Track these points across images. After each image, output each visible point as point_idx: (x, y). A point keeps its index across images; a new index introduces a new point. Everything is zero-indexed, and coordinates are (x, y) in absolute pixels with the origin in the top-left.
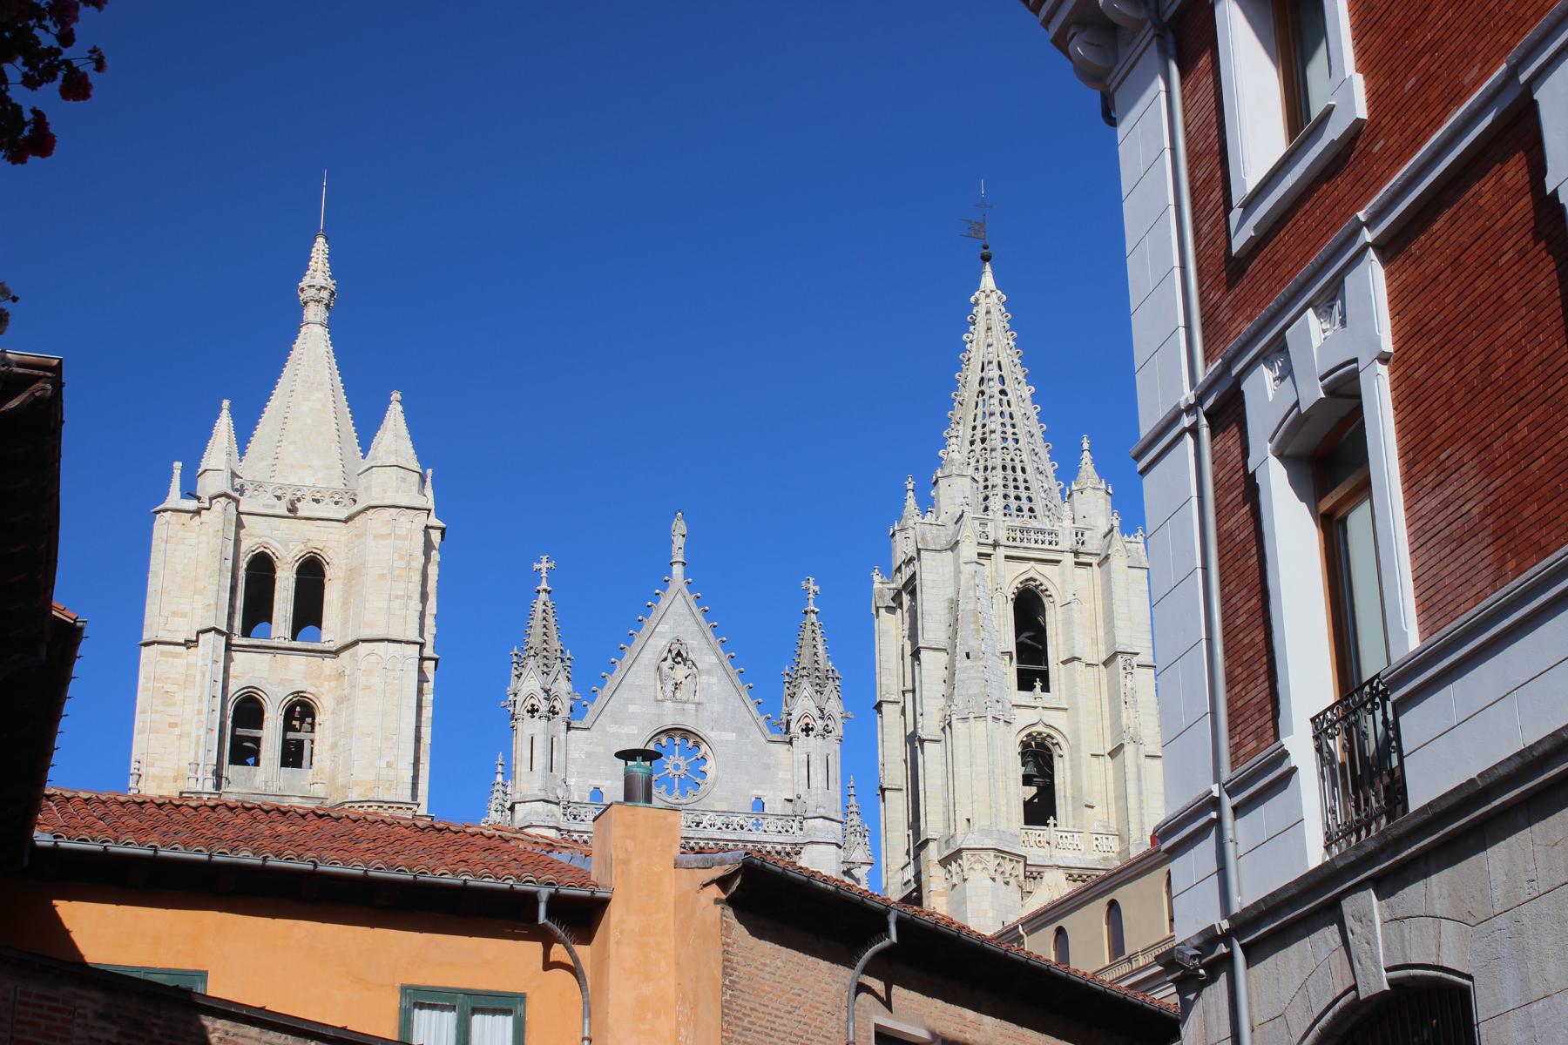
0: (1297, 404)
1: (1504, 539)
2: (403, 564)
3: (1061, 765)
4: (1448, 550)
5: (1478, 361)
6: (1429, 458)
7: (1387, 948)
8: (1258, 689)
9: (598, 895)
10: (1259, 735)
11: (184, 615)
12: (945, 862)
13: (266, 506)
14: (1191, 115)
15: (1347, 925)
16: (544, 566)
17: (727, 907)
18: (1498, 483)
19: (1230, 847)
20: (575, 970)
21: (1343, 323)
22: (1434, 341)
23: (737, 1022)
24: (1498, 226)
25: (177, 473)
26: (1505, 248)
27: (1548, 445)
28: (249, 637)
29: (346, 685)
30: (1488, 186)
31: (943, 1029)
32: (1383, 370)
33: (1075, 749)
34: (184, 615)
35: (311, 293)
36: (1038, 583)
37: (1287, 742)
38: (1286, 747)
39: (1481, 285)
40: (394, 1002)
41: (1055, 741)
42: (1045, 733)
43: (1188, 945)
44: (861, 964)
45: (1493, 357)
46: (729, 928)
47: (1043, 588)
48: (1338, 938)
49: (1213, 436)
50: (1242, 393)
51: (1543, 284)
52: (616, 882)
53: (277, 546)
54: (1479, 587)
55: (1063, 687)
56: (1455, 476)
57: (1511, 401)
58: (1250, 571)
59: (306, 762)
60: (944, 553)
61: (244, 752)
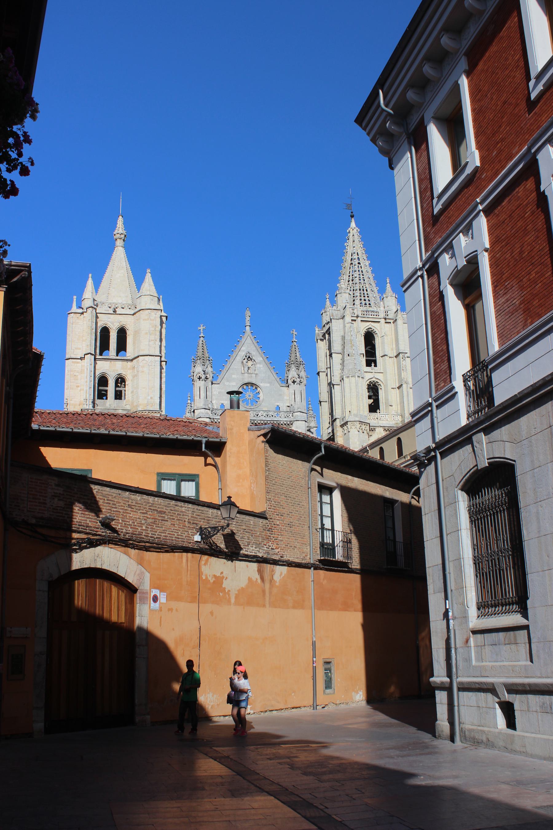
0: (457, 266)
1: (527, 312)
4: (508, 316)
5: (518, 250)
6: (502, 284)
7: (487, 452)
8: (444, 365)
9: (222, 440)
11: (80, 349)
12: (342, 426)
13: (105, 310)
14: (419, 165)
15: (474, 445)
16: (201, 328)
18: (525, 293)
19: (435, 419)
20: (215, 466)
21: (472, 238)
22: (503, 244)
23: (271, 482)
24: (525, 203)
25: (75, 300)
26: (527, 211)
27: (542, 279)
30: (521, 189)
31: (341, 483)
32: (486, 254)
33: (386, 386)
34: (80, 349)
35: (118, 236)
37: (454, 383)
39: (519, 224)
40: (155, 478)
44: (312, 461)
45: (523, 249)
47: (374, 331)
48: (471, 449)
49: (428, 278)
50: (438, 263)
51: (540, 223)
53: (110, 324)
54: (519, 329)
55: (381, 365)
56: (510, 291)
57: (529, 264)
58: (441, 325)
59: (123, 398)
60: (340, 320)
61: (102, 395)
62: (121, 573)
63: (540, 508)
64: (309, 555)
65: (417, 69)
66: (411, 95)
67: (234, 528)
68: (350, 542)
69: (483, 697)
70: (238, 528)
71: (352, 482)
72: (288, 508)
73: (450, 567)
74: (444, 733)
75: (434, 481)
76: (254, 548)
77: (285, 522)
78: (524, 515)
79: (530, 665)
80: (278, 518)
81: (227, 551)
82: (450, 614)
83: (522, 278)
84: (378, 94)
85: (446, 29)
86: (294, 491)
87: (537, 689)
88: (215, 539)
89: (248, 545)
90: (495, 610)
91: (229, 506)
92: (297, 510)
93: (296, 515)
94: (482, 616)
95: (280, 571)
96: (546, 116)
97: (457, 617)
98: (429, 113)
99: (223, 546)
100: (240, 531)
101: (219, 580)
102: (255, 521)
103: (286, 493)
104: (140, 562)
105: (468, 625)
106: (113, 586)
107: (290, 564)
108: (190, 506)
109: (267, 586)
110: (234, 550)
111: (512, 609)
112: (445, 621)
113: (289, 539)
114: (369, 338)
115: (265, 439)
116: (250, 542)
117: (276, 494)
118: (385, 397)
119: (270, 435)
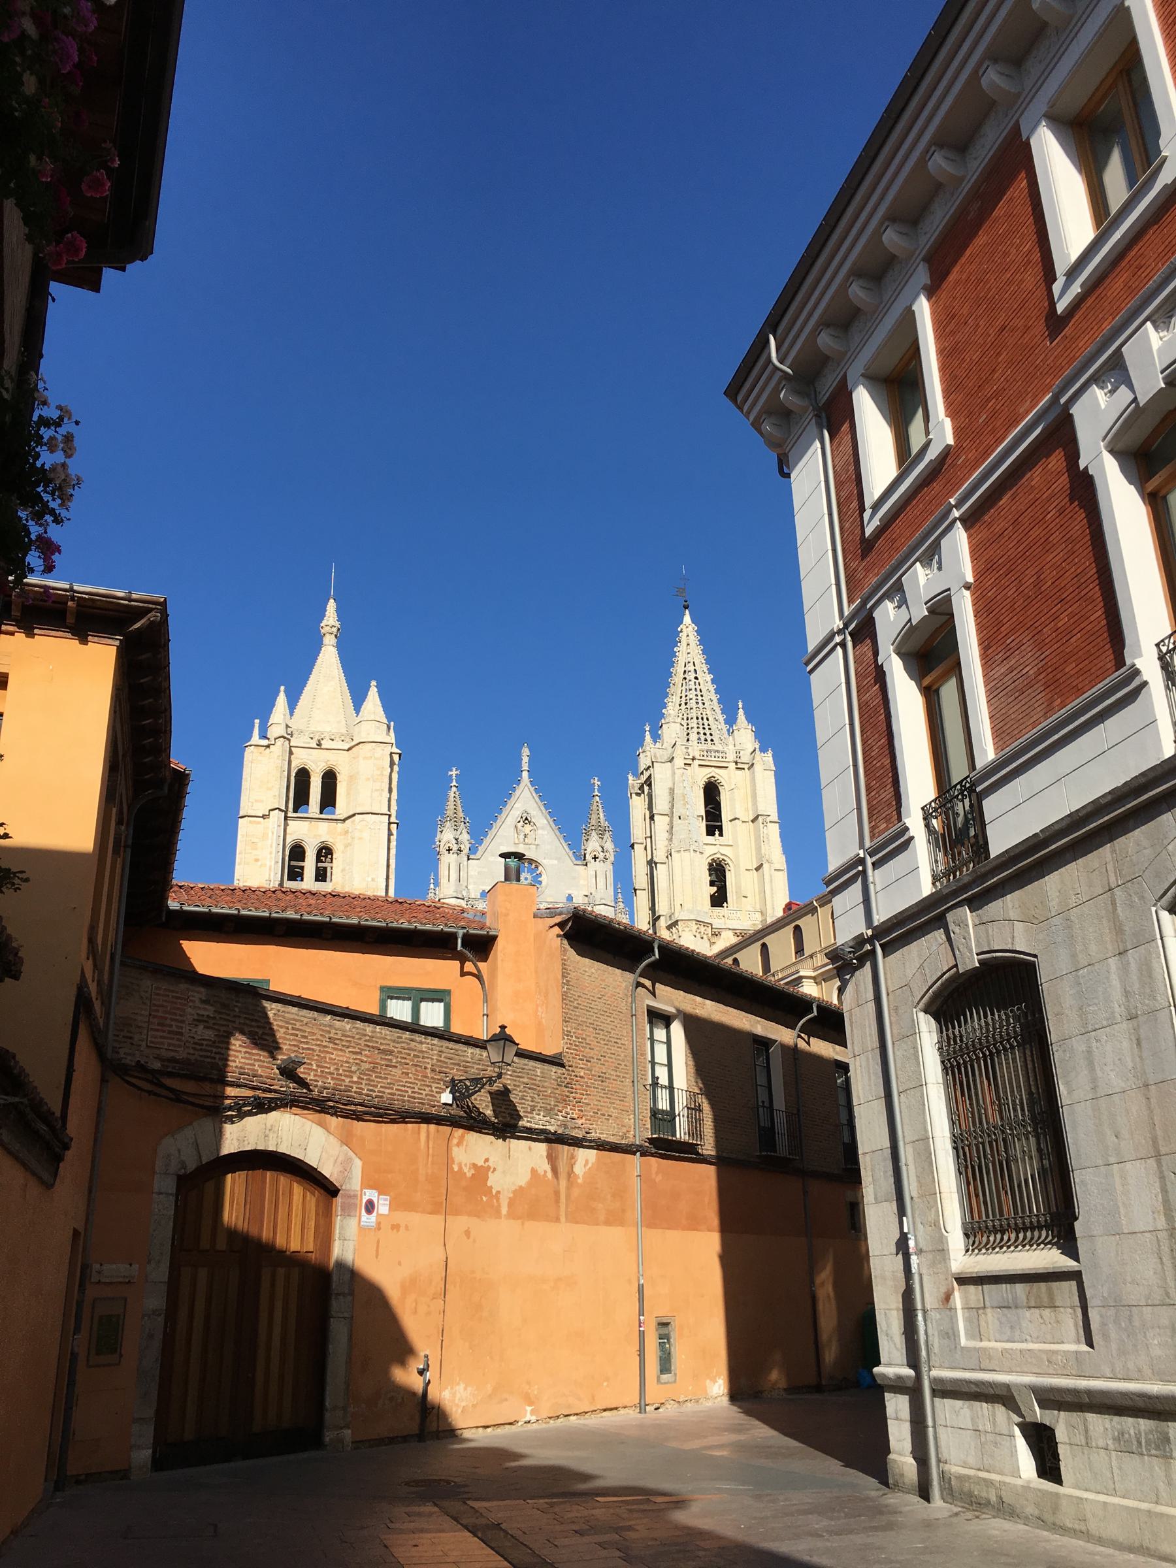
0: (910, 620)
2: (379, 773)
4: (1013, 697)
5: (1031, 580)
6: (1000, 643)
10: (888, 820)
11: (261, 801)
13: (304, 743)
14: (837, 461)
15: (950, 928)
16: (454, 773)
18: (1047, 653)
19: (871, 887)
20: (479, 977)
21: (940, 569)
22: (1001, 572)
26: (1050, 509)
27: (1082, 626)
28: (297, 812)
29: (349, 837)
30: (1037, 473)
31: (684, 1008)
32: (967, 593)
34: (261, 801)
37: (908, 821)
38: (907, 825)
39: (1034, 534)
40: (376, 995)
43: (846, 945)
44: (639, 970)
45: (1042, 577)
46: (565, 950)
48: (944, 937)
49: (854, 647)
51: (1077, 528)
53: (312, 764)
56: (1017, 652)
59: (328, 879)
61: (295, 874)
62: (312, 1159)
63: (1094, 1044)
65: (837, 291)
66: (825, 340)
67: (509, 1082)
69: (985, 1411)
70: (515, 1081)
73: (907, 1154)
74: (906, 1481)
75: (870, 995)
76: (541, 1117)
77: (593, 1073)
78: (1058, 1056)
79: (1088, 1353)
80: (582, 1066)
81: (496, 1121)
82: (911, 1243)
83: (1040, 628)
84: (768, 341)
85: (892, 218)
86: (609, 1019)
87: (1107, 1401)
88: (476, 1099)
90: (1002, 1239)
92: (613, 1052)
94: (973, 1250)
95: (585, 1158)
96: (1086, 338)
97: (924, 1249)
98: (856, 369)
99: (489, 1112)
100: (519, 1086)
101: (481, 1173)
102: (544, 1069)
103: (595, 1023)
104: (346, 1140)
105: (948, 1268)
106: (295, 1184)
107: (601, 1146)
108: (436, 1041)
109: (563, 1183)
110: (508, 1119)
111: (1039, 1238)
112: (900, 1256)
113: (600, 1101)
114: (711, 792)
118: (736, 883)
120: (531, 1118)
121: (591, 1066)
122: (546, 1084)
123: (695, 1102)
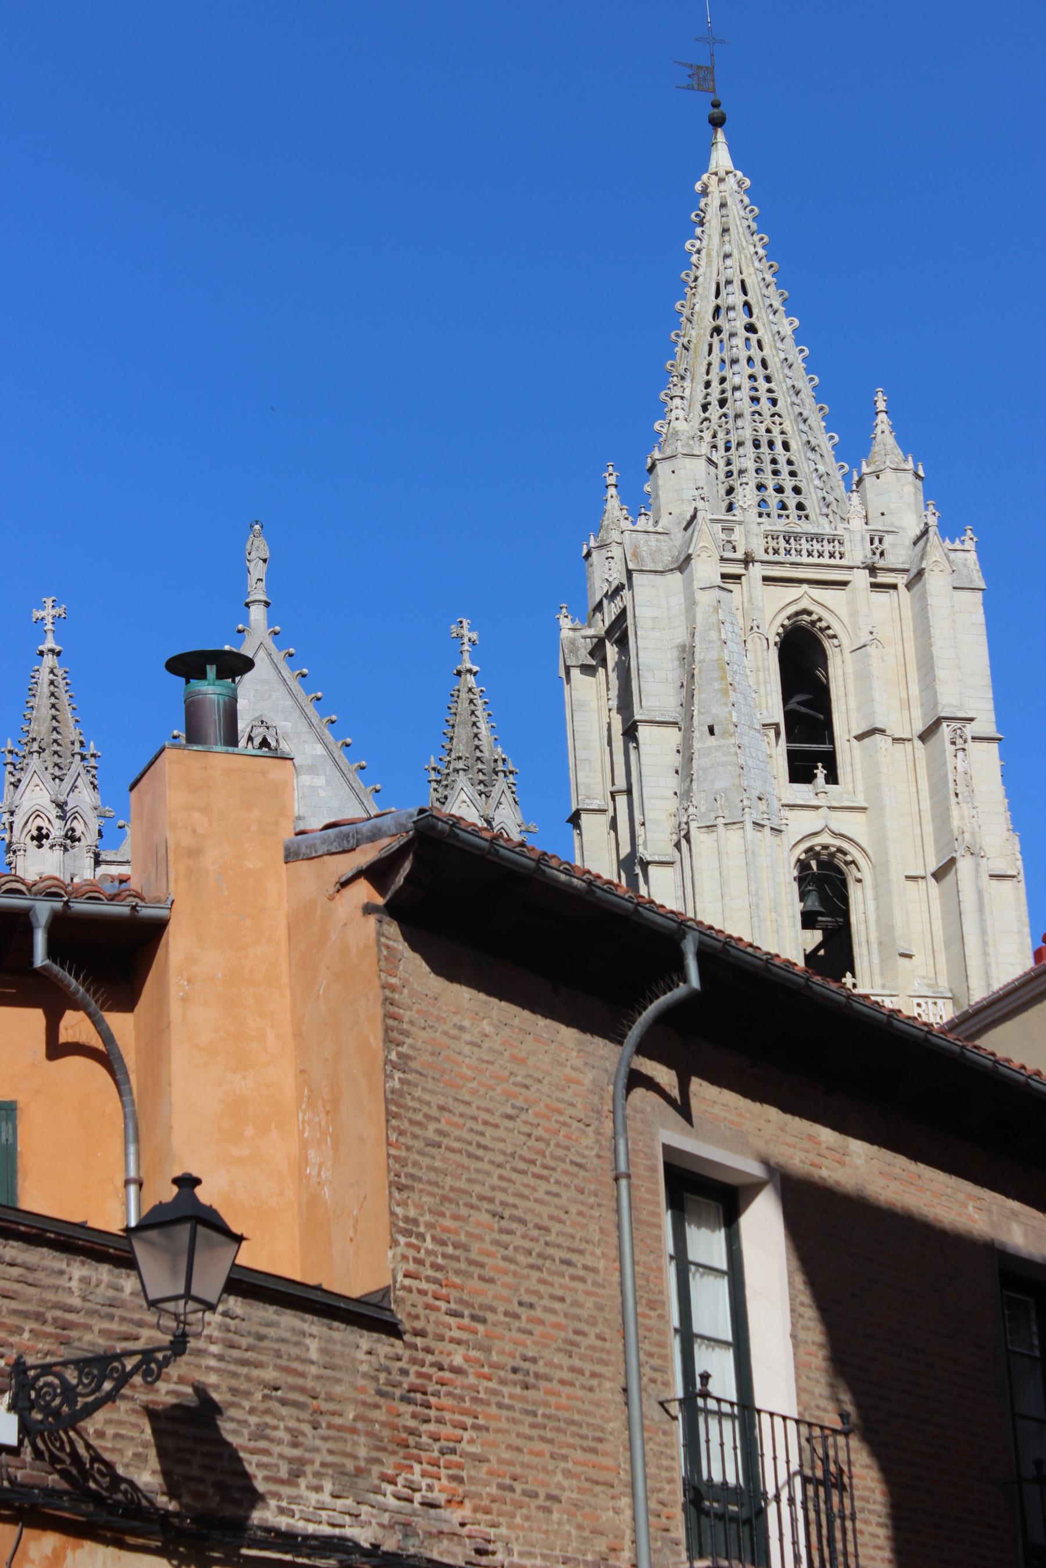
3: (860, 894)
9: (145, 912)
16: (48, 613)
17: (387, 919)
23: (417, 1130)
31: (782, 1160)
33: (881, 869)
36: (814, 617)
41: (849, 858)
42: (834, 846)
44: (635, 1032)
46: (392, 958)
47: (823, 624)
52: (178, 889)
55: (859, 775)
60: (669, 577)
64: (627, 1543)
67: (212, 1379)
68: (842, 1488)
70: (235, 1375)
71: (841, 1163)
72: (509, 1279)
76: (326, 1497)
77: (495, 1357)
80: (457, 1334)
81: (173, 1506)
86: (543, 1186)
88: (100, 1434)
89: (296, 1475)
91: (187, 1227)
92: (559, 1293)
93: (553, 1318)
100: (248, 1394)
102: (331, 1340)
103: (499, 1196)
110: (214, 1502)
113: (519, 1450)
115: (382, 892)
116: (302, 1462)
117: (444, 1199)
119: (407, 867)
120: (292, 1500)
121: (487, 1336)
122: (338, 1389)
123: (825, 1460)
